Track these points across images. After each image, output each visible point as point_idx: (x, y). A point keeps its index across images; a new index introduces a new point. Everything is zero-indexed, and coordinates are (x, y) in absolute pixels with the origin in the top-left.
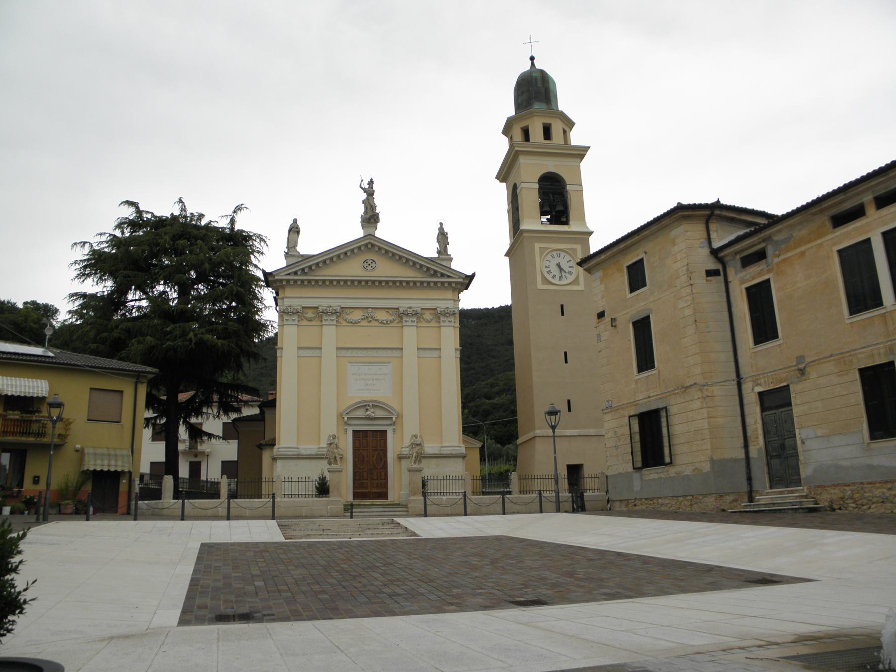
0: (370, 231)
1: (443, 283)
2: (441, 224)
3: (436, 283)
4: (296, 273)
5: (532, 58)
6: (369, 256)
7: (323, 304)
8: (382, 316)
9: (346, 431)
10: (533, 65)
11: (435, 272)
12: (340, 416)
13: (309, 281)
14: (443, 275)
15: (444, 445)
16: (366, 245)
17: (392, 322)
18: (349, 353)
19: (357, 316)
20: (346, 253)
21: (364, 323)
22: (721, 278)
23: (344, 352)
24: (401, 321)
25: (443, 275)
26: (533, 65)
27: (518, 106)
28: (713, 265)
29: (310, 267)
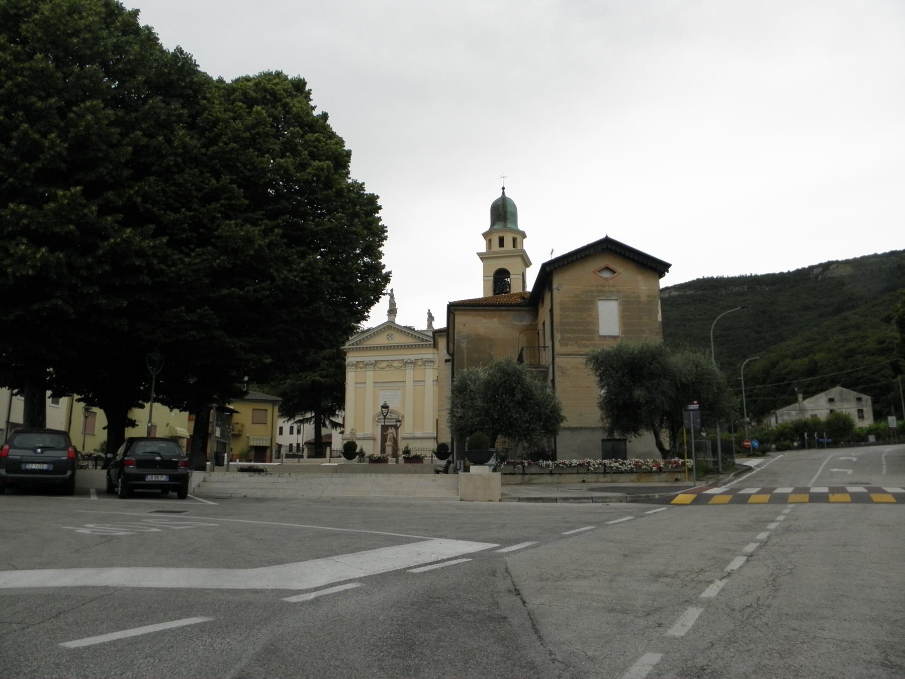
0: (392, 317)
1: (426, 345)
2: (429, 310)
3: (422, 345)
4: (353, 344)
5: (503, 189)
6: (390, 332)
7: (367, 359)
8: (396, 364)
9: (377, 425)
10: (503, 193)
11: (423, 339)
12: (374, 418)
13: (360, 348)
14: (426, 341)
15: (425, 432)
16: (388, 326)
17: (401, 367)
18: (380, 385)
19: (384, 365)
20: (377, 331)
21: (388, 368)
22: (450, 363)
23: (377, 384)
24: (405, 367)
25: (426, 341)
26: (503, 193)
27: (493, 223)
28: (448, 357)
29: (360, 340)
